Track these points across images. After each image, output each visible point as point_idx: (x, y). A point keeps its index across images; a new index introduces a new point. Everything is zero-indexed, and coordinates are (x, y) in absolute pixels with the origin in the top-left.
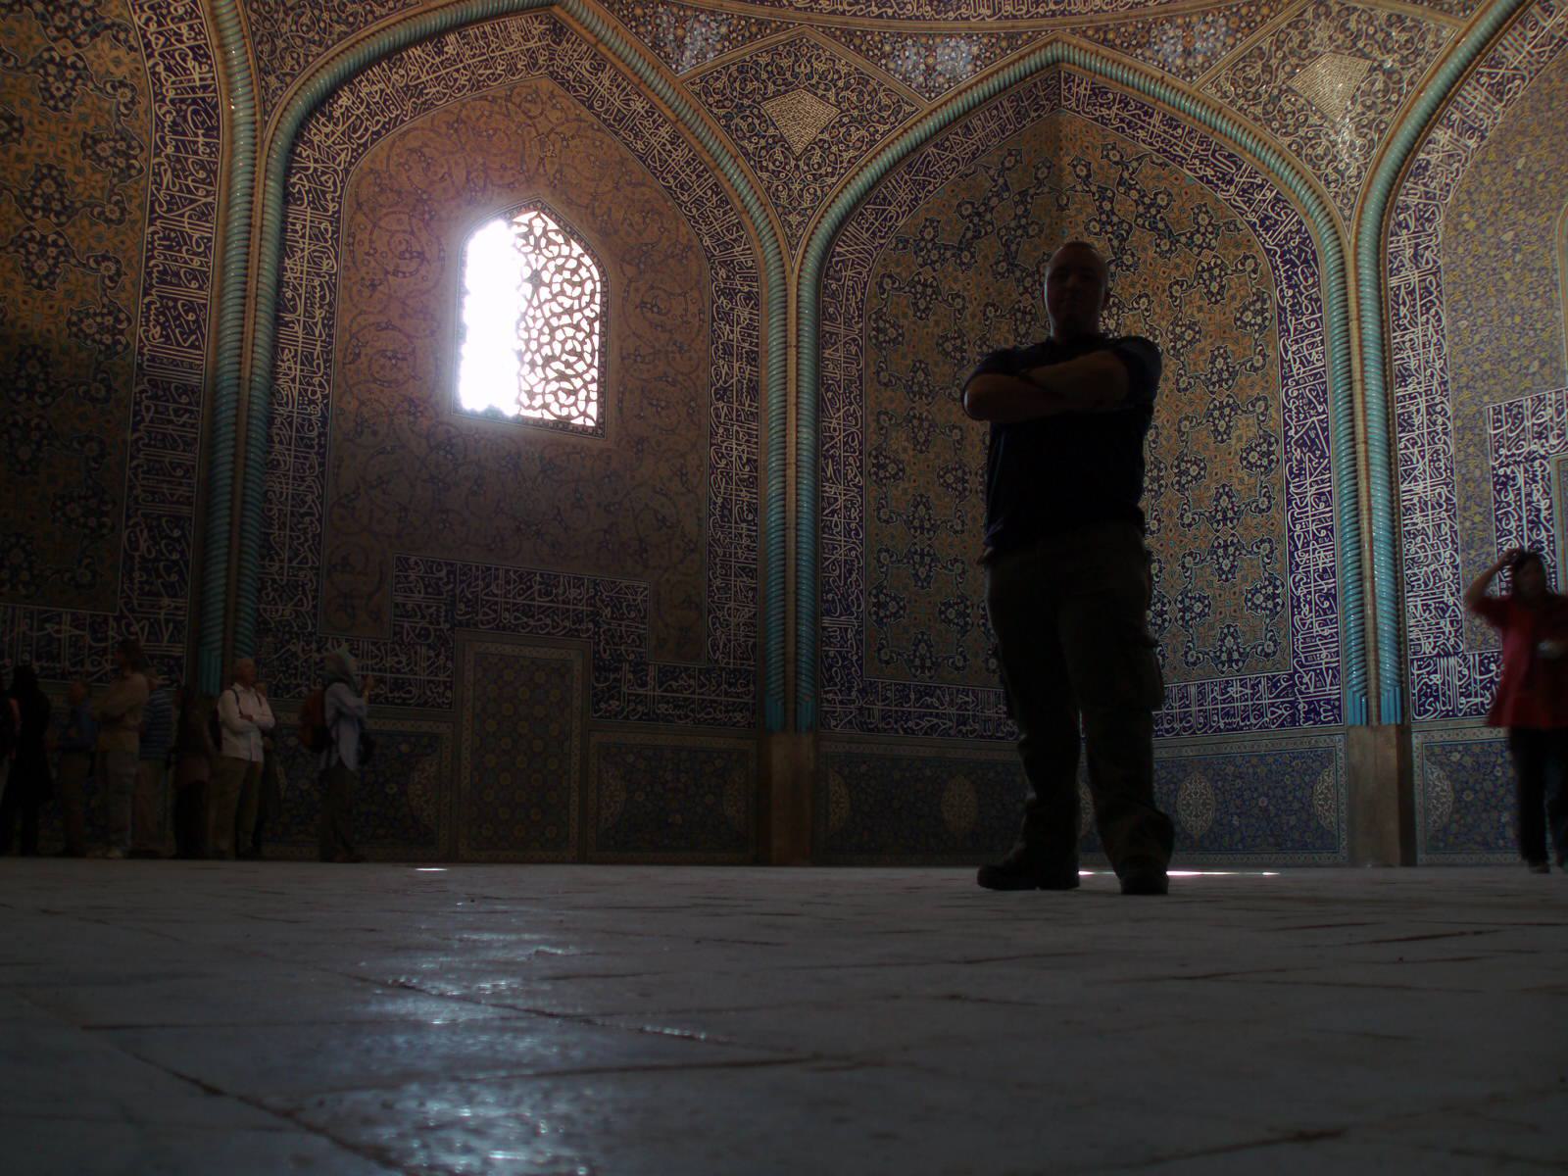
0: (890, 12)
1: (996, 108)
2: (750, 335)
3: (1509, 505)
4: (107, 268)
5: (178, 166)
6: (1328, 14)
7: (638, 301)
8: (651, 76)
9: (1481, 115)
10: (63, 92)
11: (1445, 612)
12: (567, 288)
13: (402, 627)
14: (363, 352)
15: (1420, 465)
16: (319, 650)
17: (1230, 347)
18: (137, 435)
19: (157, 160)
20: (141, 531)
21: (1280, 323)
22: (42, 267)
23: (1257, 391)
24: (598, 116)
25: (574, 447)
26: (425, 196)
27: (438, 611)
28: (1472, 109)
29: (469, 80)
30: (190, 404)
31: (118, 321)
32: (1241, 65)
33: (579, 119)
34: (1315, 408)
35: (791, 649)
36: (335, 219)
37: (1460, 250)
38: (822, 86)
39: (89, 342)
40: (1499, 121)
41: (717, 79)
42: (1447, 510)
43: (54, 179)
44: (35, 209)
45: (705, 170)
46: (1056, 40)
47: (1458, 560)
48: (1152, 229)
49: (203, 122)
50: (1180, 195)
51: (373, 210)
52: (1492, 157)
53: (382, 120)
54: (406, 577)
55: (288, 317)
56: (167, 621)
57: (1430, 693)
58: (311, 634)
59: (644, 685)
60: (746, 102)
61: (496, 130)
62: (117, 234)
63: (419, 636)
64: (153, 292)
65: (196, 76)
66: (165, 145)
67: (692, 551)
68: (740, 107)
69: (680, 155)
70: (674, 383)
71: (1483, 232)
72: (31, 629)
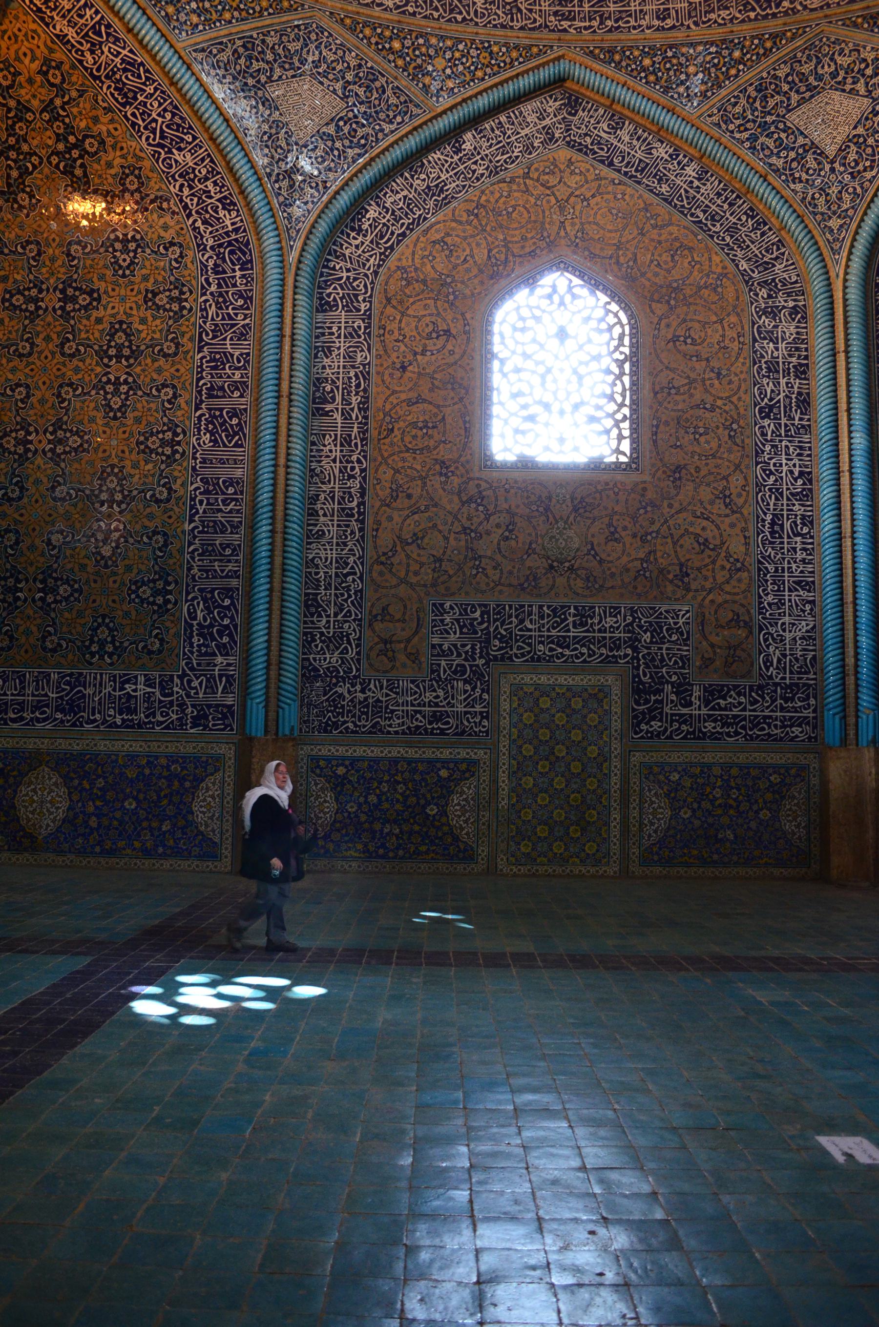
2: (797, 349)
4: (166, 394)
5: (221, 300)
7: (670, 336)
8: (665, 118)
10: (128, 261)
12: (594, 336)
13: (439, 665)
14: (396, 426)
16: (363, 691)
18: (193, 525)
19: (204, 298)
20: (198, 603)
22: (116, 403)
24: (619, 171)
25: (607, 484)
26: (449, 280)
27: (473, 648)
29: (487, 169)
30: (235, 493)
31: (176, 434)
33: (598, 178)
35: (850, 661)
36: (368, 316)
38: (849, 80)
39: (153, 455)
41: (736, 103)
43: (124, 331)
44: (110, 358)
45: (738, 197)
49: (239, 259)
51: (401, 302)
53: (406, 221)
54: (442, 621)
55: (328, 407)
56: (221, 676)
58: (355, 677)
59: (689, 704)
60: (769, 119)
61: (514, 208)
62: (172, 365)
63: (455, 672)
64: (203, 406)
65: (228, 222)
66: (209, 284)
67: (739, 570)
68: (764, 126)
69: (708, 189)
70: (712, 410)
72: (114, 690)
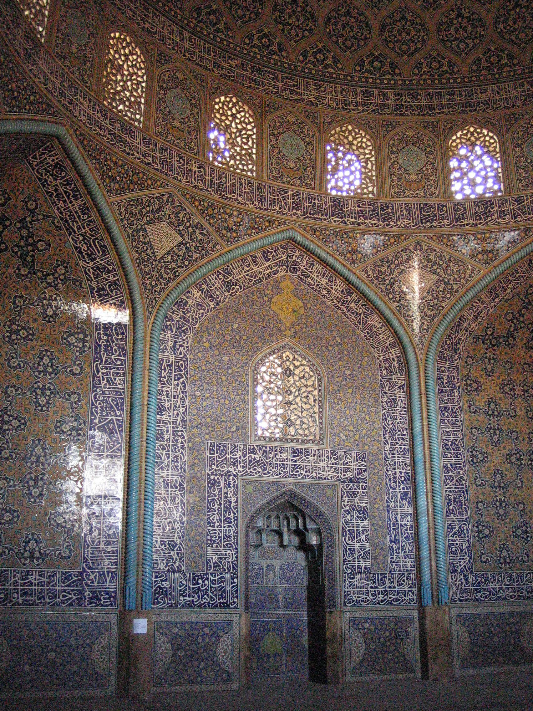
3: (215, 496)
6: (172, 202)
9: (218, 293)
11: (174, 547)
15: (166, 461)
17: (56, 353)
21: (96, 352)
23: (73, 388)
28: (213, 288)
32: (132, 203)
34: (114, 411)
37: (200, 355)
40: (227, 300)
42: (179, 490)
47: (185, 519)
48: (21, 258)
50: (55, 249)
52: (221, 316)
57: (160, 592)
71: (213, 351)
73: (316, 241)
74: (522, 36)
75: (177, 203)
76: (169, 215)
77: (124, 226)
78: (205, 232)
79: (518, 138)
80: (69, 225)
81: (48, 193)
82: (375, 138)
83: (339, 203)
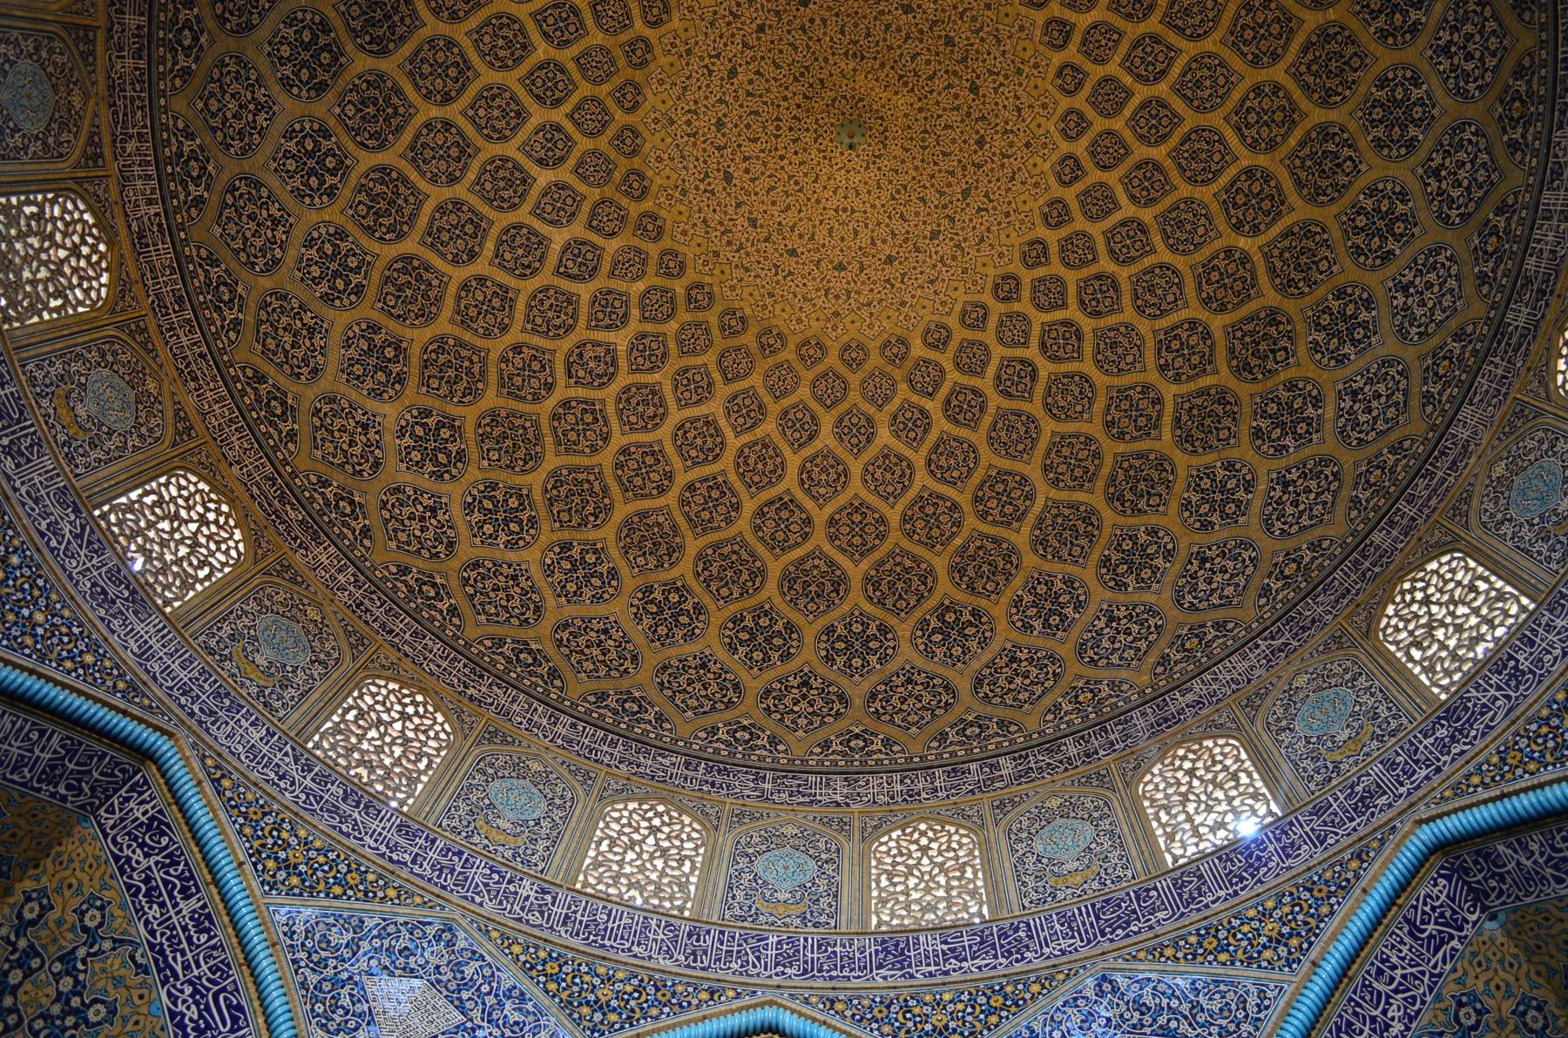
0: (54, 543)
1: (42, 733)
6: (450, 944)
32: (331, 920)
46: (171, 735)
73: (836, 1021)
74: (1229, 591)
75: (461, 944)
76: (438, 967)
77: (294, 961)
78: (529, 1006)
79: (1278, 720)
80: (166, 958)
81: (129, 887)
82: (977, 827)
83: (897, 945)
